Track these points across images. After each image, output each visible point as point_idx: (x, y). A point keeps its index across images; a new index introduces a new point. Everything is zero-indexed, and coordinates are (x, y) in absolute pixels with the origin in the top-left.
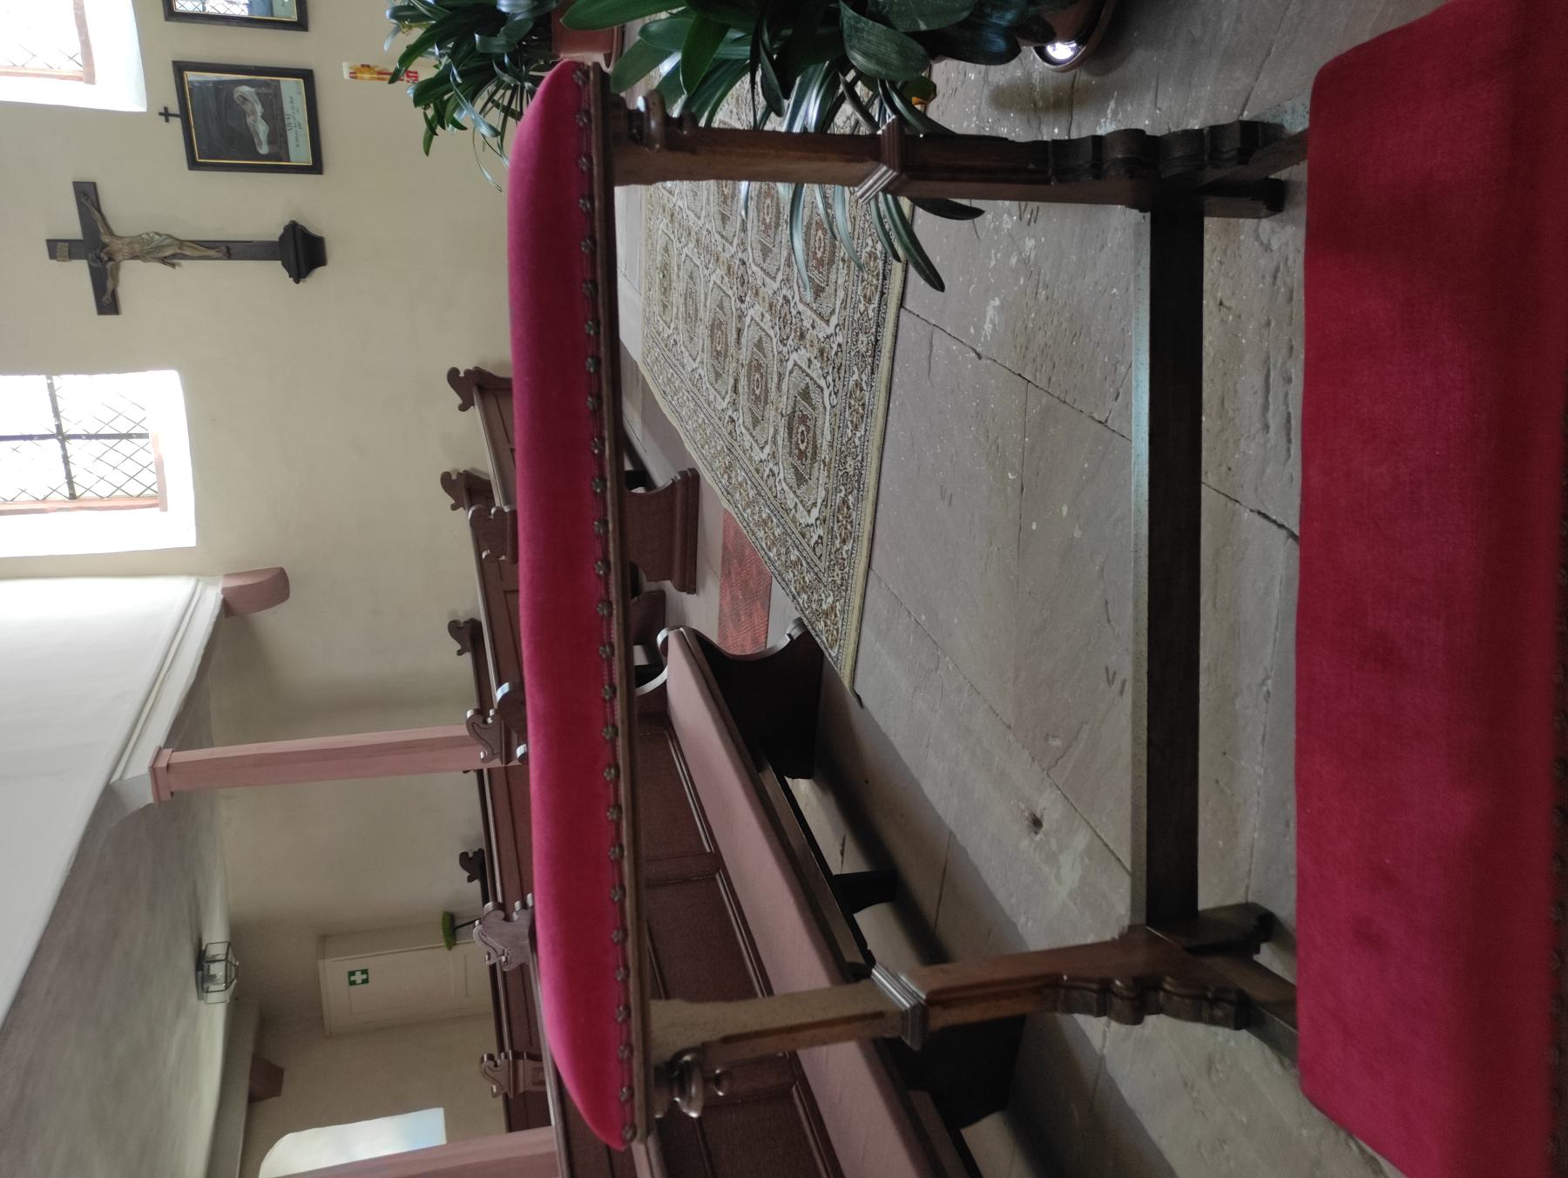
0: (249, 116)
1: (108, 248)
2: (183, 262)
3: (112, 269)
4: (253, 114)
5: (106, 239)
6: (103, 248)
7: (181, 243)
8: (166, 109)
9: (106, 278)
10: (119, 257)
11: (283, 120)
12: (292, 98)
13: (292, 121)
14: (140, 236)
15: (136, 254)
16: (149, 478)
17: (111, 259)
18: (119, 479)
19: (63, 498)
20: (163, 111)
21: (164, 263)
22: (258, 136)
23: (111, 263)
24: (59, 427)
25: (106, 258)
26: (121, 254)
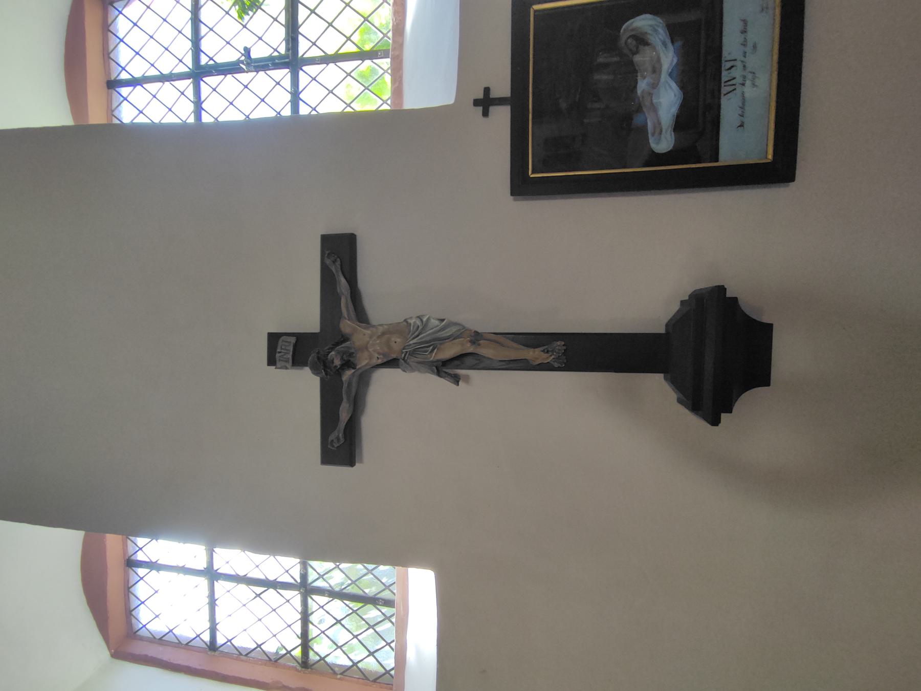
0: (644, 77)
1: (347, 344)
3: (349, 384)
4: (654, 71)
5: (347, 325)
6: (337, 344)
7: (476, 337)
8: (487, 90)
9: (342, 400)
10: (363, 362)
12: (745, 22)
13: (737, 73)
14: (405, 320)
15: (394, 356)
16: (389, 662)
17: (348, 364)
18: (358, 654)
19: (296, 664)
20: (480, 95)
21: (439, 373)
23: (348, 374)
24: (304, 576)
25: (337, 362)
26: (366, 354)
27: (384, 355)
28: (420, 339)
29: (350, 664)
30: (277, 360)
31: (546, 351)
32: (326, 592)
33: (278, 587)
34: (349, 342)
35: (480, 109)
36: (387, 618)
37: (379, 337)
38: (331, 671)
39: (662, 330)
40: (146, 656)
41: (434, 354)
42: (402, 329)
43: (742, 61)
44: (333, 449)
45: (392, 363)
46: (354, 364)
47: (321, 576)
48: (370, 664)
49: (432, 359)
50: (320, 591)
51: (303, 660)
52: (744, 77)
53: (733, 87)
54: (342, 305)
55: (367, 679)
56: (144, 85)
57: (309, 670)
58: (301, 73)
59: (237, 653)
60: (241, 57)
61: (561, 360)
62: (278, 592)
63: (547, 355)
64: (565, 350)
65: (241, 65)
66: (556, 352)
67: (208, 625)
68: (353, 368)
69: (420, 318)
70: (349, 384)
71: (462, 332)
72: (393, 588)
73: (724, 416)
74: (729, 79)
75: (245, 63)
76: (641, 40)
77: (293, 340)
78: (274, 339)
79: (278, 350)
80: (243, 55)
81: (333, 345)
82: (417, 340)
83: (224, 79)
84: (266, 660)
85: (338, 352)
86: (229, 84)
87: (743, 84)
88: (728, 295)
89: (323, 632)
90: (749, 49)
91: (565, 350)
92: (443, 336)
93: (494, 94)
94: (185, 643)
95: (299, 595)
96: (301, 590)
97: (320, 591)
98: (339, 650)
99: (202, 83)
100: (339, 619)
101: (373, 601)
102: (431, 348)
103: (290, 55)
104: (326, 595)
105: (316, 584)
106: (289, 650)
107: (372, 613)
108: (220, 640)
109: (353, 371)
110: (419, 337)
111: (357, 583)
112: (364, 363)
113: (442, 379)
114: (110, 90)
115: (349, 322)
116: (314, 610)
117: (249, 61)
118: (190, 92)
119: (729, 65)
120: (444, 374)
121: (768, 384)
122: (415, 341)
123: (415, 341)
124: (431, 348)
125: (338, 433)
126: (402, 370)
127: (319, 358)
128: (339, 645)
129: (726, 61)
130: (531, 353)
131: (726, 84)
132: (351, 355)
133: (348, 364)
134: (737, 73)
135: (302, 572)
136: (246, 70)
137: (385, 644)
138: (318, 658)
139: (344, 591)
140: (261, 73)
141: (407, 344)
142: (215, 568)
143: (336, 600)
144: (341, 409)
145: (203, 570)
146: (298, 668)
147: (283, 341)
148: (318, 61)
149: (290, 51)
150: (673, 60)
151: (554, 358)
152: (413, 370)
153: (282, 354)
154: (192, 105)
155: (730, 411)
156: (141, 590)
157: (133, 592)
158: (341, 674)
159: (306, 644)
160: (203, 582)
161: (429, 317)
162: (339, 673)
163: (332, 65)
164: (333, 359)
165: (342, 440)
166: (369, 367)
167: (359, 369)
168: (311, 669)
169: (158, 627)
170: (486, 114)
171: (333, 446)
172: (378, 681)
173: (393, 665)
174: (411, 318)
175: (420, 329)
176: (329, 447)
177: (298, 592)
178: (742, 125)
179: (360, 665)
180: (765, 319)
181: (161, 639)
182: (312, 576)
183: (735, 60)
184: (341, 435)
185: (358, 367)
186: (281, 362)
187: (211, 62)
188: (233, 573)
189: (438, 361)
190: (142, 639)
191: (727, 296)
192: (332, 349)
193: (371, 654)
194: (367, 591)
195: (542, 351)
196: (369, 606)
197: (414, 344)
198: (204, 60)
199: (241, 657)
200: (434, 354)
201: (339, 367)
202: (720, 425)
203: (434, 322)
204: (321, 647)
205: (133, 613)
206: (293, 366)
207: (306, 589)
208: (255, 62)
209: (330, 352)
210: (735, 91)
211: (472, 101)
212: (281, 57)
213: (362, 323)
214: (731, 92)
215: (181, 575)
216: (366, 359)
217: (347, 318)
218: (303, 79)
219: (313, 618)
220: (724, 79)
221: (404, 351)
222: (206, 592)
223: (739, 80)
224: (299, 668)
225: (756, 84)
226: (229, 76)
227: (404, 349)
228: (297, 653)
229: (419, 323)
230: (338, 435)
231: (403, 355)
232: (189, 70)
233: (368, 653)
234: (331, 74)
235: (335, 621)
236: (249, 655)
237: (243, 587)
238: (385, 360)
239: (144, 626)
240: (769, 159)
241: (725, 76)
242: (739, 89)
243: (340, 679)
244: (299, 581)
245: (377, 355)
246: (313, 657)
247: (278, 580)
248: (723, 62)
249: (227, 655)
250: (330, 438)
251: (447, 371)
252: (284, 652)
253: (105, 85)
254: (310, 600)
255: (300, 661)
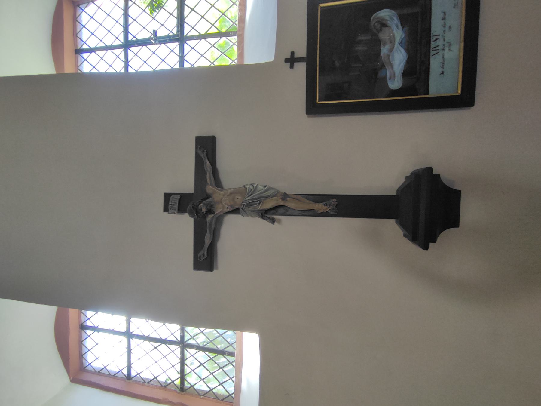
1: (210, 200)
2: (282, 218)
3: (211, 223)
5: (210, 189)
7: (285, 196)
8: (293, 53)
9: (206, 232)
10: (219, 210)
11: (429, 42)
12: (444, 13)
13: (440, 43)
14: (244, 186)
15: (237, 207)
16: (231, 389)
17: (210, 211)
18: (213, 384)
19: (177, 389)
20: (289, 56)
21: (263, 217)
22: (391, 65)
23: (210, 217)
24: (182, 337)
25: (204, 210)
26: (221, 205)
27: (231, 206)
28: (252, 197)
29: (208, 389)
30: (169, 208)
31: (326, 205)
32: (195, 347)
33: (167, 343)
34: (211, 199)
35: (289, 64)
36: (230, 363)
37: (228, 196)
38: (197, 394)
39: (395, 194)
40: (90, 381)
41: (260, 205)
42: (242, 191)
43: (442, 36)
44: (200, 260)
45: (235, 211)
46: (213, 211)
47: (192, 338)
48: (220, 390)
49: (259, 209)
50: (192, 346)
51: (181, 386)
52: (444, 45)
53: (438, 51)
54: (207, 177)
55: (218, 398)
56: (96, 52)
57: (185, 392)
58: (185, 45)
59: (143, 381)
60: (151, 36)
61: (334, 211)
62: (167, 346)
63: (326, 207)
64: (337, 204)
65: (152, 40)
66: (332, 206)
67: (126, 364)
68: (214, 214)
69: (252, 185)
70: (211, 223)
71: (277, 193)
72: (235, 345)
73: (431, 244)
74: (435, 46)
75: (153, 39)
76: (383, 25)
77: (179, 197)
78: (167, 196)
79: (170, 203)
80: (152, 35)
81: (202, 200)
82: (250, 198)
83: (142, 48)
84: (160, 386)
85: (204, 204)
86: (144, 52)
87: (444, 50)
88: (434, 173)
89: (193, 370)
90: (447, 29)
91: (337, 204)
92: (265, 195)
93: (297, 56)
94: (113, 375)
95: (179, 348)
96: (181, 345)
97: (192, 346)
98: (202, 381)
99: (129, 50)
100: (202, 363)
101: (222, 353)
102: (259, 202)
103: (179, 35)
104: (195, 348)
105: (189, 342)
106: (173, 380)
107: (222, 360)
108: (133, 374)
109: (213, 215)
110: (251, 196)
111: (213, 342)
112: (219, 211)
113: (264, 220)
114: (77, 55)
115: (211, 187)
116: (188, 357)
117: (156, 38)
118: (122, 56)
119: (435, 38)
120: (266, 218)
121: (458, 226)
122: (249, 198)
123: (249, 198)
124: (259, 202)
125: (204, 251)
126: (241, 215)
127: (193, 207)
128: (202, 378)
129: (433, 36)
130: (317, 206)
131: (433, 49)
132: (212, 206)
133: (210, 211)
134: (440, 43)
135: (181, 335)
136: (154, 43)
137: (229, 378)
138: (189, 386)
139: (205, 346)
140: (163, 45)
141: (244, 200)
142: (131, 331)
143: (201, 351)
144: (205, 237)
145: (124, 332)
146: (178, 391)
147: (173, 198)
148: (195, 38)
149: (180, 32)
150: (402, 36)
151: (330, 209)
152: (248, 215)
153: (172, 205)
154: (123, 63)
155: (435, 241)
156: (88, 343)
157: (84, 344)
158: (203, 395)
159: (183, 376)
160: (124, 339)
161: (257, 185)
162: (201, 395)
163: (203, 40)
164: (202, 208)
165: (206, 256)
166: (223, 213)
167: (216, 214)
168: (185, 392)
169: (97, 365)
170: (292, 67)
171: (201, 259)
172: (224, 400)
173: (233, 391)
174: (247, 185)
175: (252, 190)
176: (198, 259)
177: (179, 346)
178: (442, 73)
179: (214, 391)
180: (456, 188)
181: (99, 372)
182: (187, 337)
183: (439, 35)
184: (205, 253)
185: (216, 213)
186: (172, 210)
187: (134, 39)
188: (141, 334)
189: (262, 210)
190: (88, 371)
191: (433, 173)
192: (201, 202)
193: (221, 384)
194: (219, 346)
195: (324, 205)
196: (220, 356)
197: (248, 200)
198: (130, 38)
199: (145, 384)
200: (260, 205)
201: (205, 213)
202: (429, 249)
203: (260, 187)
204: (191, 379)
205: (84, 356)
206: (178, 212)
207: (183, 344)
208: (159, 39)
209: (200, 204)
210: (438, 53)
211: (284, 59)
212: (174, 36)
213: (217, 187)
214: (436, 54)
215: (112, 335)
216: (221, 208)
217: (210, 184)
218: (187, 48)
219: (187, 362)
220: (432, 46)
221: (243, 204)
222: (126, 345)
223: (441, 47)
224: (178, 391)
225: (451, 49)
226: (144, 47)
227: (243, 203)
228: (178, 382)
229: (251, 187)
230: (204, 253)
231: (242, 206)
232: (121, 43)
233: (219, 384)
234: (203, 45)
235: (200, 364)
236: (150, 383)
237: (147, 342)
238: (232, 209)
239: (90, 364)
240: (459, 93)
241: (433, 44)
242: (441, 53)
243: (201, 398)
244: (179, 340)
245: (227, 206)
246: (187, 385)
247: (167, 339)
248: (432, 35)
249: (137, 383)
250: (199, 255)
251: (267, 216)
252: (170, 381)
253: (74, 52)
254: (185, 351)
255: (179, 387)
